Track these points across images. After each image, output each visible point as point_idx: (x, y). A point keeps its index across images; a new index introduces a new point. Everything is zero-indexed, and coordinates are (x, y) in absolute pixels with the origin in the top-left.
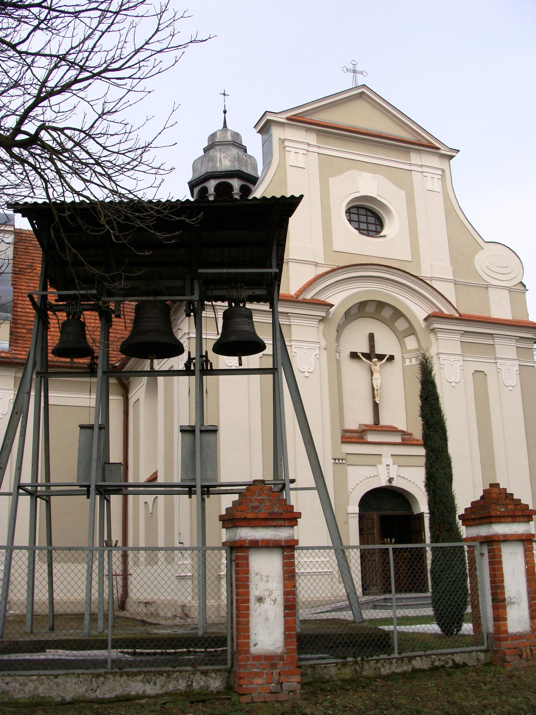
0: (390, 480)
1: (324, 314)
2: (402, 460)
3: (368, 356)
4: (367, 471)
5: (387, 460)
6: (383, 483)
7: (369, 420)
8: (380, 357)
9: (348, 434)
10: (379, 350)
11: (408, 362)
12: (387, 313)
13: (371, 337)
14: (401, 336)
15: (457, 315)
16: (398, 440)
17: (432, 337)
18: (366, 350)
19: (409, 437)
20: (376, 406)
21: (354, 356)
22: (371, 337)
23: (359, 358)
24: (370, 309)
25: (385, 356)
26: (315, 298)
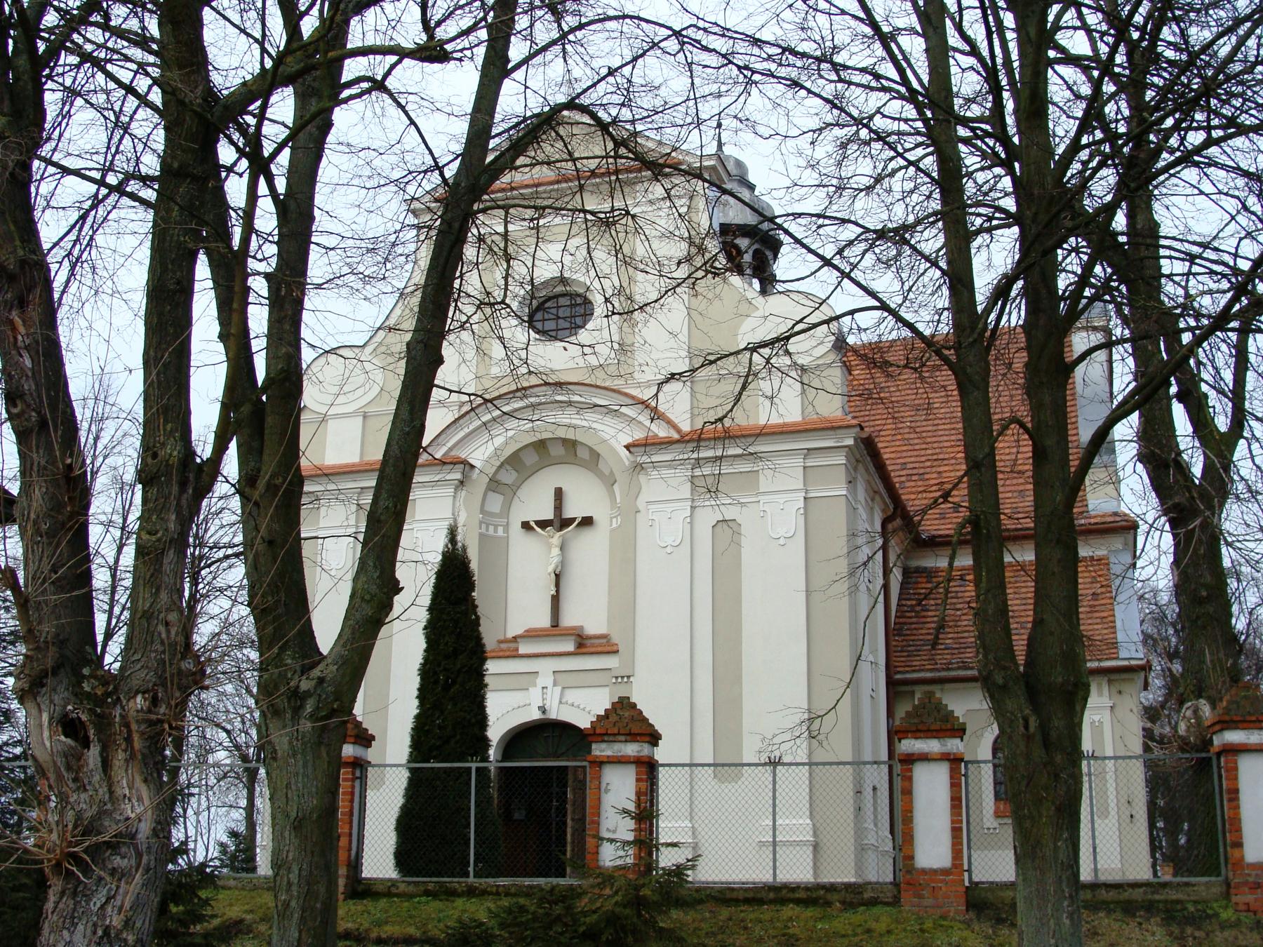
0: (543, 710)
1: (458, 476)
2: (570, 679)
3: (543, 524)
4: (516, 698)
5: (546, 679)
6: (536, 715)
7: (544, 621)
8: (565, 523)
9: (503, 646)
10: (569, 513)
11: (614, 525)
12: (583, 453)
13: (559, 494)
14: (609, 481)
15: (676, 436)
16: (570, 647)
17: (642, 478)
18: (549, 515)
19: (604, 641)
20: (556, 600)
21: (526, 525)
22: (559, 494)
23: (531, 529)
24: (557, 451)
25: (574, 519)
26: (453, 453)
